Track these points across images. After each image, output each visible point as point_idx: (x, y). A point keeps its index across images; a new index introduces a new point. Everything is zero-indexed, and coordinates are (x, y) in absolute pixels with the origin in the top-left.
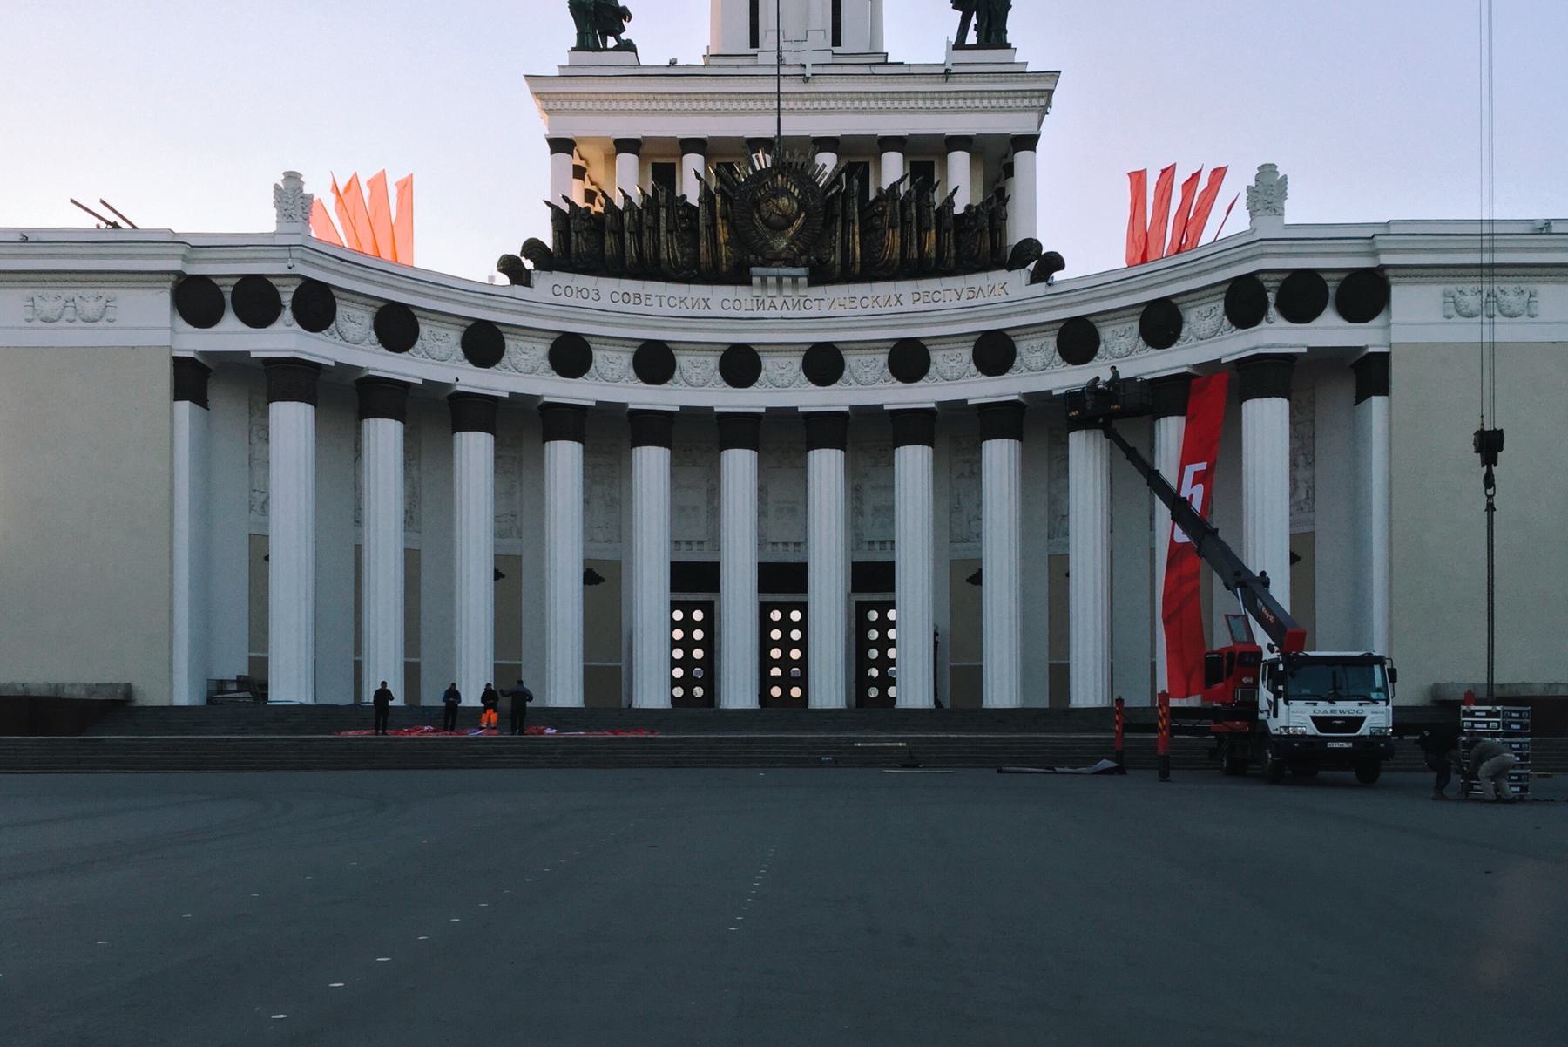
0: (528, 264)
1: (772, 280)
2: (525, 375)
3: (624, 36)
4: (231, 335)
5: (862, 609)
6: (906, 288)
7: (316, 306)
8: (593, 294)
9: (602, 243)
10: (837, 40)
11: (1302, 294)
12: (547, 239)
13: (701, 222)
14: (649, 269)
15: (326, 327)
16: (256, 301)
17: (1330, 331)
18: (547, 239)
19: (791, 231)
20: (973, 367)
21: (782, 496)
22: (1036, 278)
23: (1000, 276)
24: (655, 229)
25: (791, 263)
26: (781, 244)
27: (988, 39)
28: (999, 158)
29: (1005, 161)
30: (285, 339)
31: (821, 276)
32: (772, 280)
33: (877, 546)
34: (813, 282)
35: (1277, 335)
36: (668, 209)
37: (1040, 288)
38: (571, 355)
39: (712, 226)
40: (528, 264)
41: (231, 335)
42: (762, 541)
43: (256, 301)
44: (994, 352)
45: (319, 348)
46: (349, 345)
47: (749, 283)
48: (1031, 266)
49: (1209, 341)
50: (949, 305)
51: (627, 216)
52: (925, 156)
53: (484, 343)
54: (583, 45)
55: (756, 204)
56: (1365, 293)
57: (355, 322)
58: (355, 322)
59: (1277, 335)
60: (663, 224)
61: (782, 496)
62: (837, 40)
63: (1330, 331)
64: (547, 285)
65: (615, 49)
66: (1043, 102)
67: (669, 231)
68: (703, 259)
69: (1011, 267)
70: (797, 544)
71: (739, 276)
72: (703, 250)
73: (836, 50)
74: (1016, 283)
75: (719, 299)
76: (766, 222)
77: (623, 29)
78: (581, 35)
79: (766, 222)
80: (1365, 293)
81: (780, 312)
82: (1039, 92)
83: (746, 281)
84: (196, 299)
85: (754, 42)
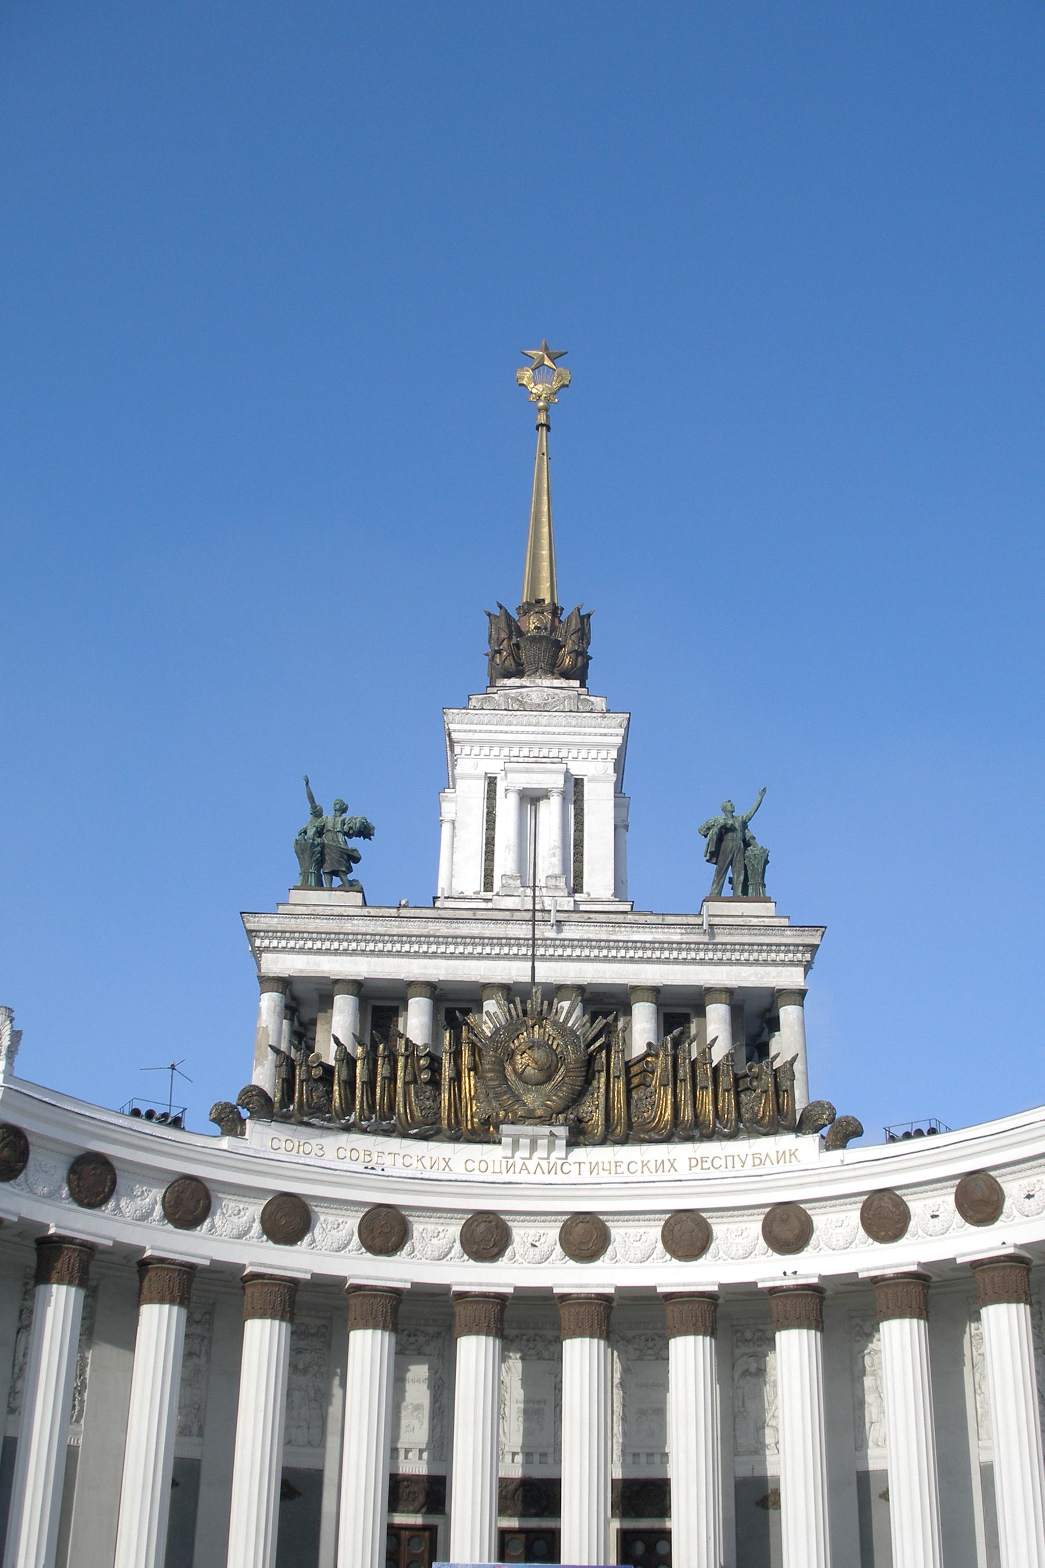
0: (245, 1113)
1: (525, 1142)
3: (350, 877)
6: (681, 1152)
8: (316, 1150)
9: (332, 1091)
13: (447, 1071)
15: (15, 1177)
19: (548, 1087)
20: (762, 1243)
23: (787, 1141)
24: (392, 1078)
25: (546, 1120)
27: (745, 892)
29: (768, 1016)
32: (525, 1142)
33: (643, 1459)
34: (572, 1143)
36: (407, 1058)
37: (836, 1155)
39: (457, 1079)
40: (245, 1113)
44: (787, 1227)
47: (500, 1143)
48: (825, 1131)
50: (738, 1173)
51: (359, 1063)
52: (678, 1010)
55: (511, 1055)
60: (400, 1073)
62: (577, 887)
64: (260, 1136)
65: (340, 889)
66: (808, 957)
67: (406, 1084)
68: (444, 1114)
70: (543, 1455)
71: (484, 1133)
72: (445, 1103)
73: (578, 897)
76: (520, 1076)
77: (350, 870)
78: (305, 874)
79: (520, 1076)
81: (532, 1173)
85: (488, 885)
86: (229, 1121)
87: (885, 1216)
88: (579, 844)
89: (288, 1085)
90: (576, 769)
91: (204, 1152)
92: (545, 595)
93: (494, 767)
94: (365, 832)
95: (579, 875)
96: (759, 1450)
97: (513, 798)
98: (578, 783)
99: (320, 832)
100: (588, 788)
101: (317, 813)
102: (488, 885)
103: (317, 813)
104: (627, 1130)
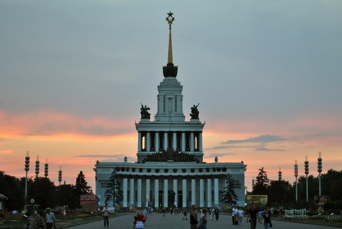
2: (145, 173)
4: (120, 172)
5: (179, 196)
6: (184, 163)
7: (128, 170)
10: (176, 111)
11: (219, 170)
12: (147, 158)
14: (157, 160)
16: (123, 169)
17: (221, 173)
18: (147, 158)
21: (171, 184)
22: (197, 163)
26: (171, 158)
28: (198, 134)
30: (125, 173)
31: (175, 161)
35: (217, 173)
37: (197, 164)
38: (149, 170)
41: (120, 172)
42: (168, 188)
43: (123, 169)
44: (192, 170)
45: (128, 173)
46: (130, 173)
49: (211, 173)
53: (141, 170)
54: (142, 118)
56: (224, 169)
57: (131, 170)
58: (131, 170)
59: (217, 173)
61: (171, 184)
62: (176, 111)
63: (221, 173)
64: (147, 163)
69: (194, 161)
71: (166, 161)
74: (195, 163)
75: (164, 164)
80: (224, 169)
81: (170, 165)
82: (202, 126)
83: (167, 161)
84: (117, 169)
86: (144, 162)
87: (201, 170)
88: (176, 105)
89: (148, 158)
90: (175, 94)
91: (141, 166)
92: (171, 62)
93: (163, 94)
94: (149, 109)
95: (176, 109)
96: (191, 188)
97: (167, 99)
98: (176, 96)
99: (144, 110)
100: (177, 97)
101: (142, 106)
102: (164, 111)
103: (142, 106)
104: (180, 161)
